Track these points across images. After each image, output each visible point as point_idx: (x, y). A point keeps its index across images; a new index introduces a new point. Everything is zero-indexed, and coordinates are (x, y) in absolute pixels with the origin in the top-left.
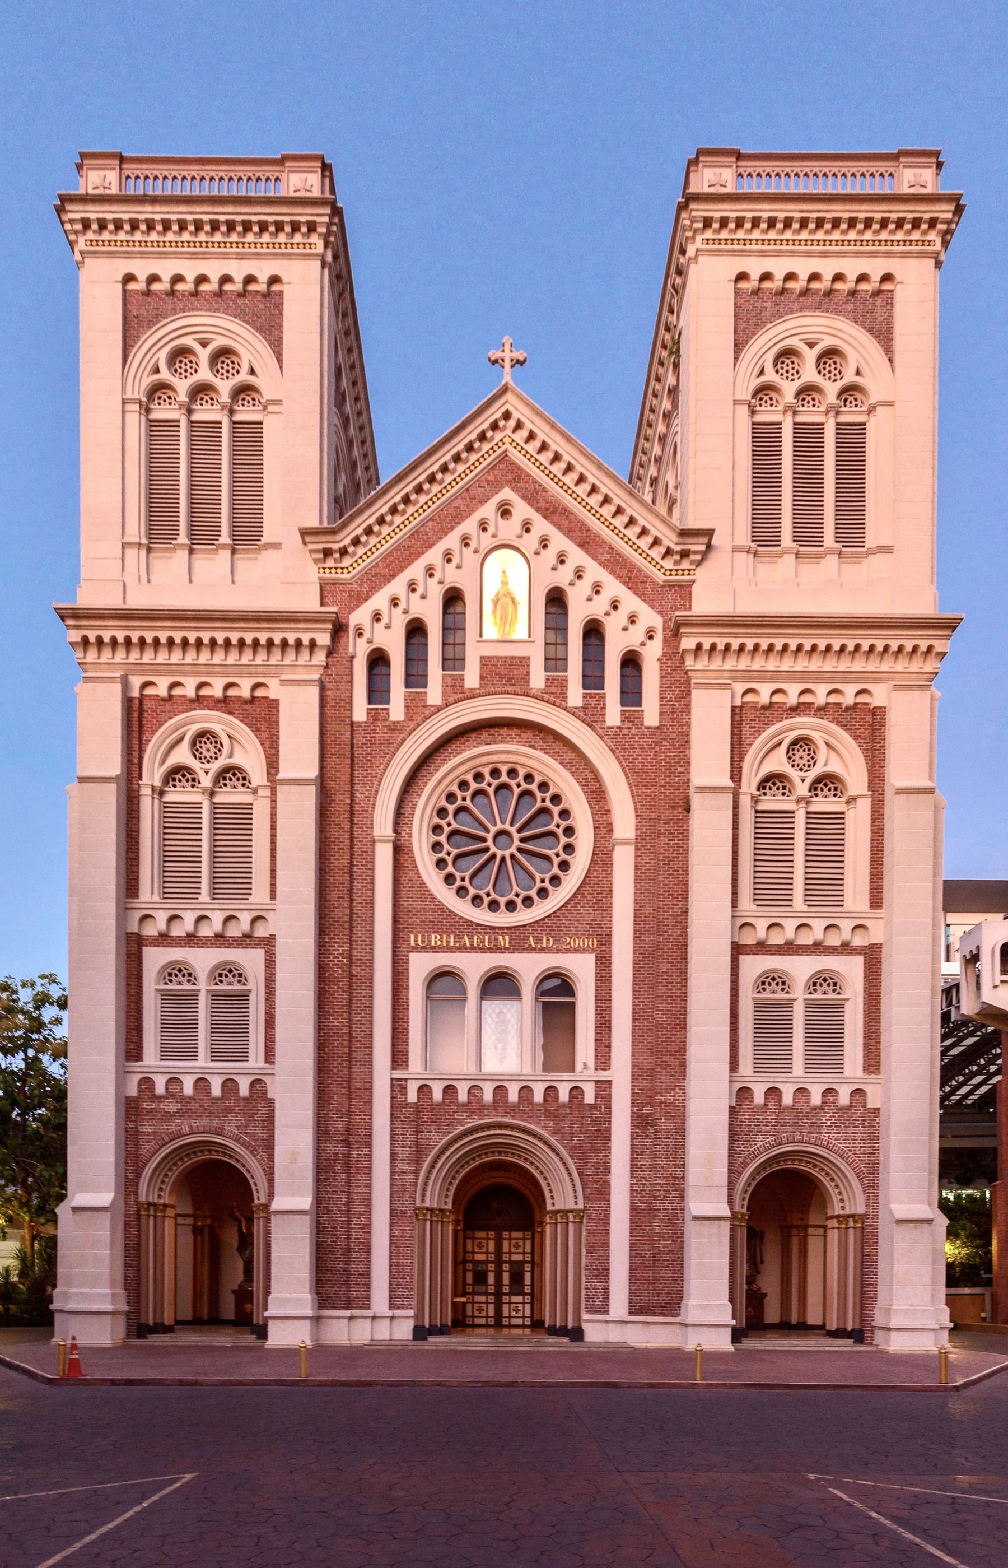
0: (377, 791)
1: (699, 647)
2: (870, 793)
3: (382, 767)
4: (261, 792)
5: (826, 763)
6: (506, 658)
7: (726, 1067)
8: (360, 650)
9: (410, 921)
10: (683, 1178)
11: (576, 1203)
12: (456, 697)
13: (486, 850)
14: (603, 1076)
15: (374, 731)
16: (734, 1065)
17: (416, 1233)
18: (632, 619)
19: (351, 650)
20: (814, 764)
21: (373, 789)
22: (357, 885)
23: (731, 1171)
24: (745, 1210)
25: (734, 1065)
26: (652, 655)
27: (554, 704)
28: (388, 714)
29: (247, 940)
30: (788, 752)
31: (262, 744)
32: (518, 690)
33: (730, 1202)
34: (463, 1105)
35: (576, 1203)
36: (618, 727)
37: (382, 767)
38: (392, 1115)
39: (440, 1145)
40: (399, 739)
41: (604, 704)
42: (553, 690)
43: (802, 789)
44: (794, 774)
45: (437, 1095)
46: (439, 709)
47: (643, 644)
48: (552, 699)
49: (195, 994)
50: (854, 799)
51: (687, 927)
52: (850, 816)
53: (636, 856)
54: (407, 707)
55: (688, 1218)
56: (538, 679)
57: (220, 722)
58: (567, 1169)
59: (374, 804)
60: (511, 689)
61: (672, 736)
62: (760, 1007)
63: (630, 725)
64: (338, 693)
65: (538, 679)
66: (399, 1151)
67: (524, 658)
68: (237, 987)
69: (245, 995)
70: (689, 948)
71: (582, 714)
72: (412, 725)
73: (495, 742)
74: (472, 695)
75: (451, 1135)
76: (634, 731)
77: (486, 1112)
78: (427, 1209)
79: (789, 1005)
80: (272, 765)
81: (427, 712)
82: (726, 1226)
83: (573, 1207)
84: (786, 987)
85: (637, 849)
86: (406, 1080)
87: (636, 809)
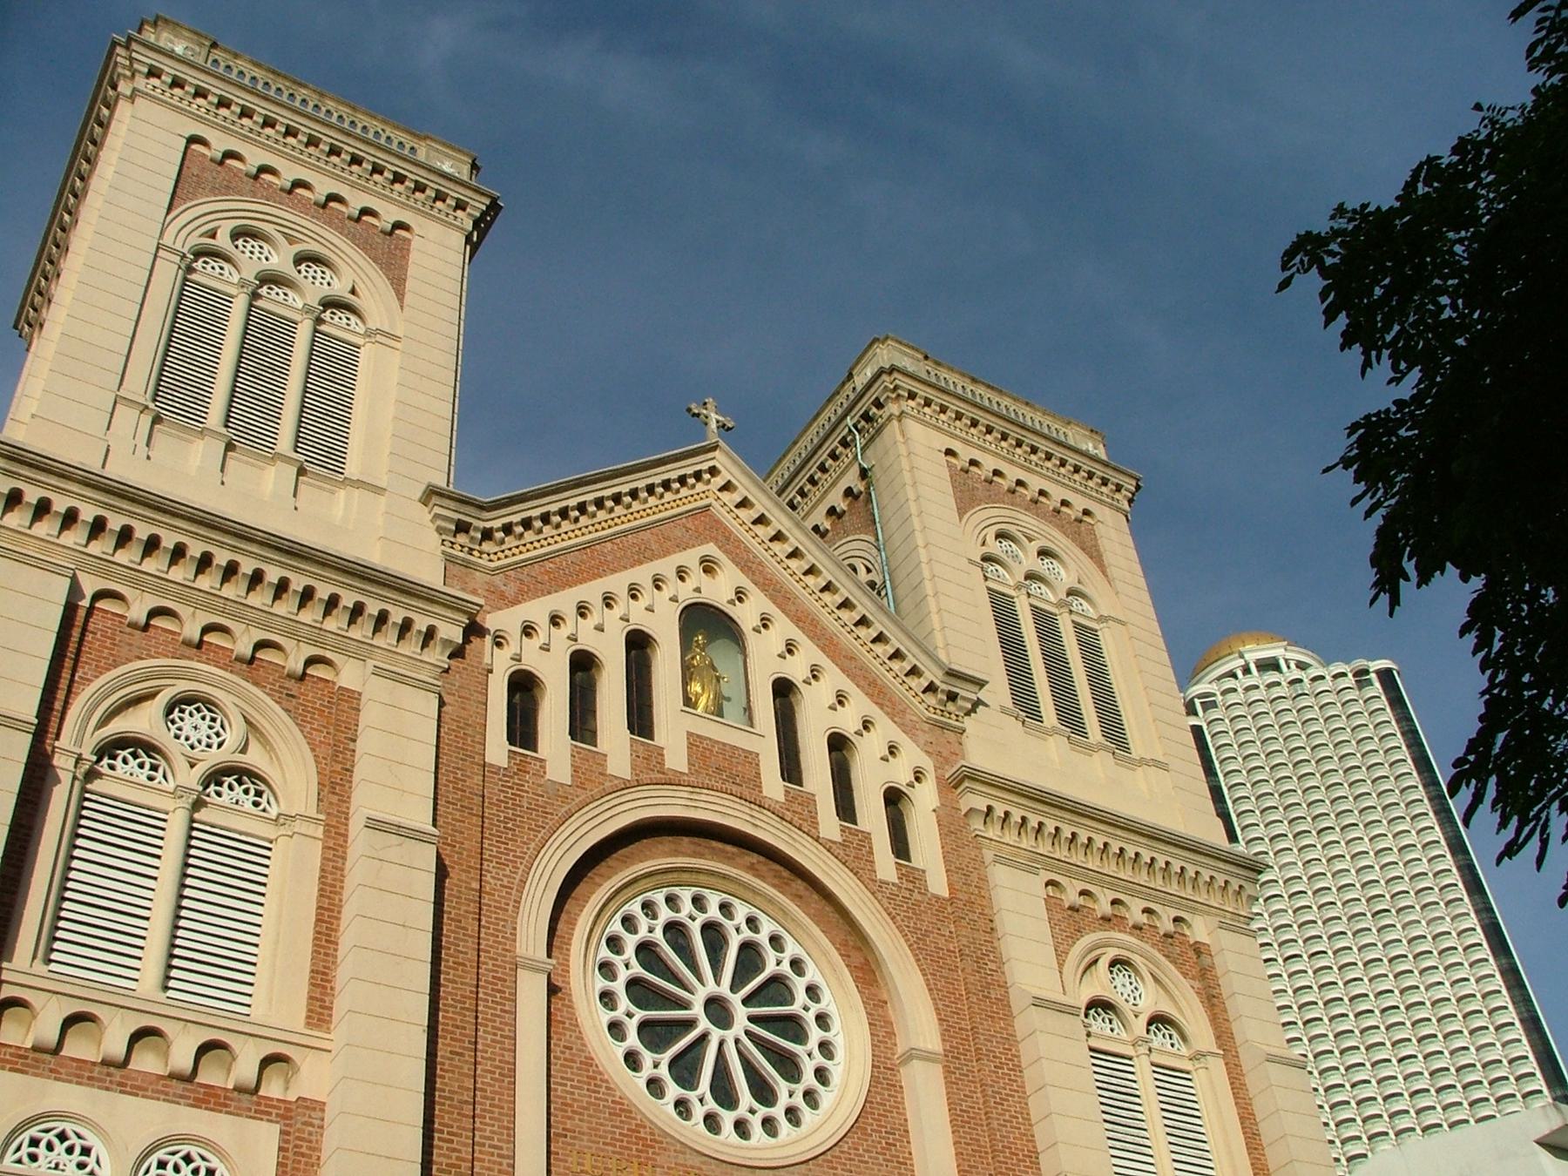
3: (532, 845)
6: (724, 744)
8: (502, 666)
19: (487, 660)
21: (518, 877)
22: (485, 1038)
28: (543, 767)
29: (245, 1097)
31: (313, 750)
32: (746, 794)
36: (893, 884)
37: (532, 845)
41: (871, 848)
42: (796, 807)
46: (626, 786)
47: (911, 785)
53: (949, 1083)
60: (735, 789)
63: (910, 886)
64: (464, 714)
67: (751, 753)
76: (916, 896)
81: (608, 784)
85: (948, 1072)
87: (937, 1009)
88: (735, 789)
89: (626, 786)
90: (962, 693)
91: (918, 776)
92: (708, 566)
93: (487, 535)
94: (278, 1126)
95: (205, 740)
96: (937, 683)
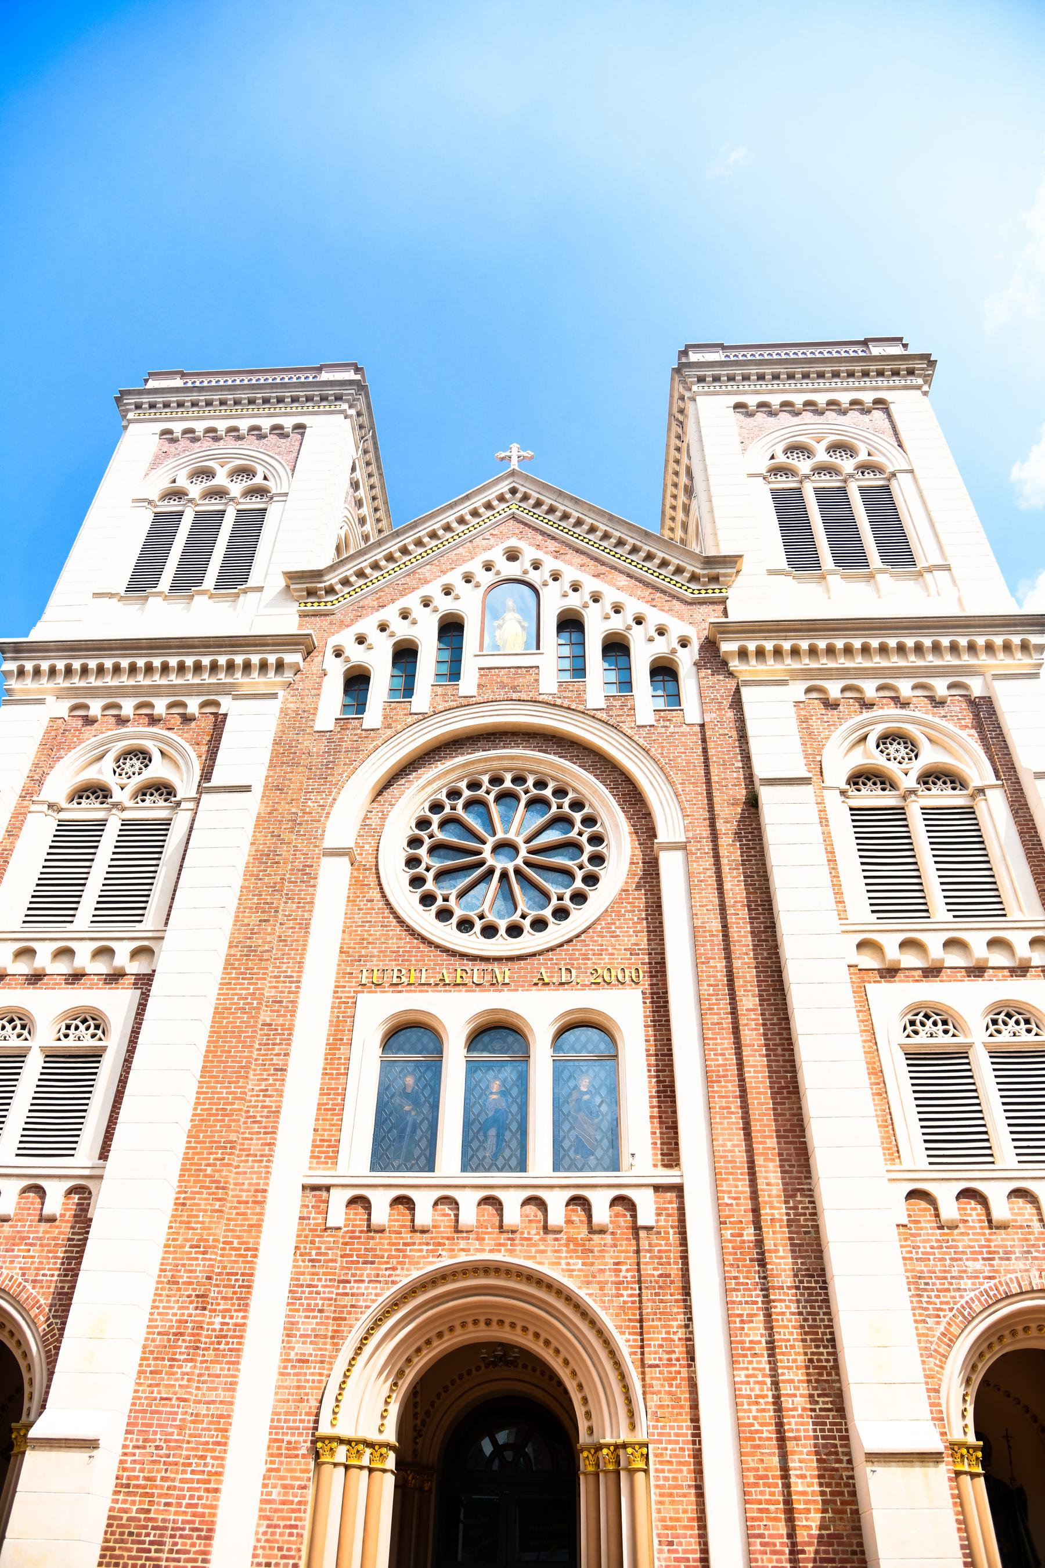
0: (334, 799)
1: (743, 654)
2: (1000, 782)
4: (184, 805)
5: (930, 756)
7: (878, 1154)
9: (363, 952)
10: (836, 1367)
11: (633, 1426)
12: (447, 705)
13: (482, 863)
14: (669, 1176)
15: (341, 739)
16: (893, 1151)
17: (310, 1493)
18: (661, 631)
20: (916, 756)
23: (926, 1352)
24: (971, 1439)
25: (893, 1151)
26: (686, 661)
27: (569, 708)
30: (878, 746)
32: (524, 696)
33: (939, 1418)
34: (423, 1232)
35: (633, 1426)
36: (651, 726)
38: (297, 1248)
39: (374, 1306)
40: (371, 746)
43: (909, 782)
44: (893, 768)
45: (381, 1213)
46: (425, 717)
48: (566, 703)
49: (20, 1056)
50: (981, 791)
51: (776, 947)
52: (981, 808)
54: (385, 717)
55: (859, 1459)
56: (549, 683)
57: (154, 738)
58: (612, 1353)
59: (328, 813)
61: (721, 732)
62: (915, 1057)
64: (303, 706)
65: (549, 683)
66: (300, 1317)
68: (88, 1042)
69: (95, 1056)
70: (784, 974)
71: (605, 715)
72: (389, 732)
73: (495, 748)
74: (467, 703)
75: (396, 1287)
77: (462, 1244)
78: (341, 1441)
79: (962, 1054)
80: (207, 774)
82: (941, 1473)
83: (624, 1437)
84: (950, 1027)
86: (328, 1188)
88: (515, 696)
89: (425, 717)
90: (721, 571)
91: (684, 643)
92: (512, 556)
93: (330, 591)
94: (139, 991)
95: (137, 770)
96: (698, 571)
